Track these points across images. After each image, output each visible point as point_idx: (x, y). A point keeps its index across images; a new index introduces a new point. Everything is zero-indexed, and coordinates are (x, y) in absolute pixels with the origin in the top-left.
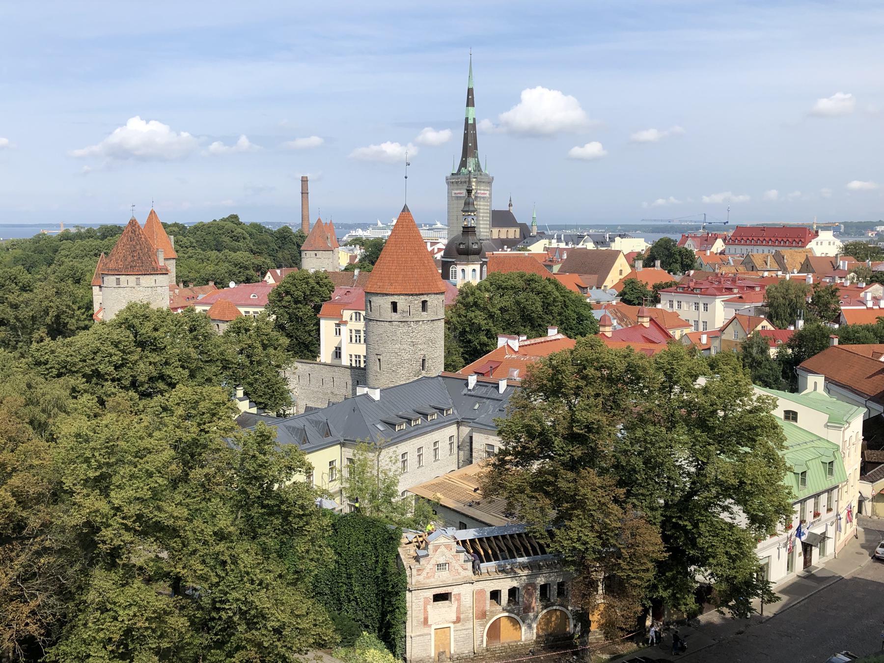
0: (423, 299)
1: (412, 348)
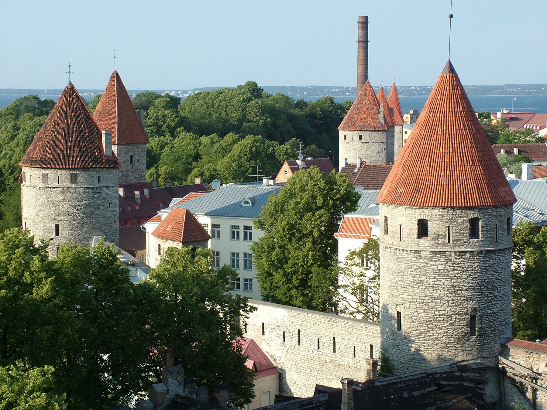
0: (471, 216)
1: (453, 295)
